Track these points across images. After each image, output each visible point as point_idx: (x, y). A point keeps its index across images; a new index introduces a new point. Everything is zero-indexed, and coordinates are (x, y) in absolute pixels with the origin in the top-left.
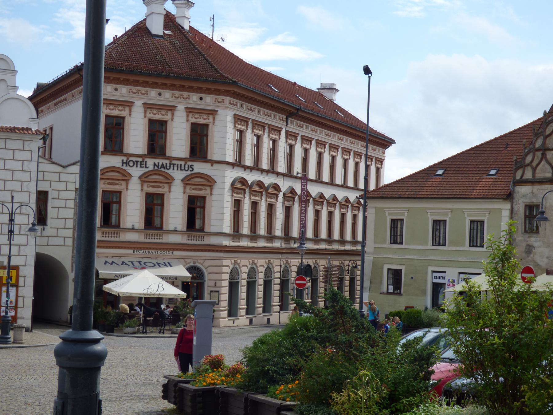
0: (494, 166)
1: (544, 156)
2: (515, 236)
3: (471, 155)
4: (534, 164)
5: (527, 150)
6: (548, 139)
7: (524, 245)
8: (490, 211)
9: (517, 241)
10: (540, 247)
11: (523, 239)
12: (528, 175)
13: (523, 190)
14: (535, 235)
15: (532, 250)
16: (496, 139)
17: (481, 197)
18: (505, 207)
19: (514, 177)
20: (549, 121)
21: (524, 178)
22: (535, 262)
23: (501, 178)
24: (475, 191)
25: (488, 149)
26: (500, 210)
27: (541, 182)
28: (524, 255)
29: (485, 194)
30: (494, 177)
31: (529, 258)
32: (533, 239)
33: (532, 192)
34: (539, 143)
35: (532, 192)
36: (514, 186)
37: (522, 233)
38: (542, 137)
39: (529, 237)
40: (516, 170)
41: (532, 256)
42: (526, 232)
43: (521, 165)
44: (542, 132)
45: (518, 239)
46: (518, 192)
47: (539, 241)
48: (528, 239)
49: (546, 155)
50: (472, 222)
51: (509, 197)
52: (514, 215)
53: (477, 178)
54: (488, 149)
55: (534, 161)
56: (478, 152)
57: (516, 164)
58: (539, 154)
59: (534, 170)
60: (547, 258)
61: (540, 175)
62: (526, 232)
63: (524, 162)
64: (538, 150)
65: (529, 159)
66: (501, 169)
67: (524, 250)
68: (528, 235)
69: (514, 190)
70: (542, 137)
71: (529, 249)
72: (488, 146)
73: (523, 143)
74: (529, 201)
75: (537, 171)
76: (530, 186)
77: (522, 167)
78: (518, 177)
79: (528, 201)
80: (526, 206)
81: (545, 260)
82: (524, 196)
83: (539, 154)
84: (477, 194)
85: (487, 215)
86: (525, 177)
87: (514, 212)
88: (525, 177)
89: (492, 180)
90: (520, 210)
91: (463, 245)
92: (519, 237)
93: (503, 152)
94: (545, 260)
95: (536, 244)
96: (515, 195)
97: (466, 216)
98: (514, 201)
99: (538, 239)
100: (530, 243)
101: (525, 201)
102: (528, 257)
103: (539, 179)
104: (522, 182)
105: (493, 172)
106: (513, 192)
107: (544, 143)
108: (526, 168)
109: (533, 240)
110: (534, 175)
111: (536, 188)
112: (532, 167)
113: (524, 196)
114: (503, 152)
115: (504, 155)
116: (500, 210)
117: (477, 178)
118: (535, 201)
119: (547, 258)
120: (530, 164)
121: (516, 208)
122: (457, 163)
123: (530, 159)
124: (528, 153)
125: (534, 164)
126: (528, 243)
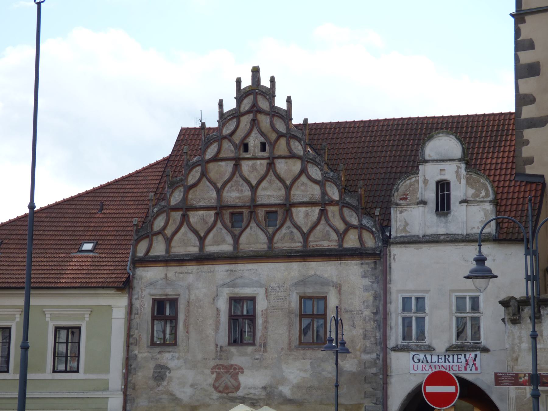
0: (87, 238)
1: (185, 218)
2: (136, 352)
3: (43, 219)
4: (169, 232)
5: (156, 210)
6: (191, 191)
7: (152, 365)
8: (92, 310)
9: (139, 359)
10: (179, 368)
11: (150, 355)
12: (159, 249)
13: (149, 274)
14: (170, 349)
15: (165, 374)
16: (80, 196)
17: (77, 285)
18: (119, 303)
19: (135, 252)
20: (194, 163)
21: (151, 254)
22: (172, 394)
23: (103, 255)
24: (64, 276)
25: (71, 211)
26: (110, 308)
27: (182, 260)
28: (152, 383)
29: (84, 280)
30: (91, 254)
31: (161, 388)
32: (167, 355)
33: (166, 278)
34: (176, 198)
35: (166, 278)
36: (135, 267)
37: (148, 347)
38: (182, 189)
39: (160, 352)
40: (138, 241)
41: (165, 383)
42: (153, 344)
43: (145, 232)
44: (182, 180)
45: (140, 356)
46: (141, 278)
47: (178, 358)
48: (159, 356)
49: (188, 216)
50: (57, 329)
51: (126, 285)
52: (133, 317)
53: (63, 255)
54: (71, 211)
55: (168, 227)
56: (53, 215)
57: (137, 231)
58: (177, 216)
59: (169, 241)
60: (192, 386)
61: (178, 249)
62: (153, 344)
63: (152, 228)
64: (175, 209)
65: (159, 223)
66: (100, 242)
67: (151, 375)
68: (158, 349)
69: (134, 275)
70: (182, 189)
71: (161, 373)
72: (69, 207)
73: (149, 198)
74: (161, 292)
75: (173, 244)
76: (161, 268)
77: (148, 237)
78: (141, 253)
79: (158, 292)
80: (154, 300)
81: (189, 391)
82: (151, 284)
83: (177, 216)
84: (69, 280)
85: (87, 316)
86: (152, 253)
87: (134, 311)
88: (152, 253)
89: (89, 259)
90: (145, 307)
91: (44, 371)
92: (142, 353)
93: (97, 216)
94: (189, 391)
95: (172, 364)
96: (135, 283)
97: (48, 319)
98: (134, 292)
99: (177, 355)
100: (162, 362)
101: (154, 292)
102: (159, 386)
103: (178, 256)
104: (148, 261)
105: (88, 246)
106: (133, 277)
107: (185, 198)
108: (154, 238)
109: (167, 357)
110: (168, 250)
111: (172, 271)
112: (165, 236)
113: (152, 284)
114: (97, 216)
115: (99, 220)
116: (110, 308)
117: (63, 255)
118: (170, 292)
119: (192, 386)
120: (161, 232)
121: (137, 304)
122: (21, 232)
123: (162, 224)
124: (158, 214)
125: (169, 232)
126: (159, 362)
